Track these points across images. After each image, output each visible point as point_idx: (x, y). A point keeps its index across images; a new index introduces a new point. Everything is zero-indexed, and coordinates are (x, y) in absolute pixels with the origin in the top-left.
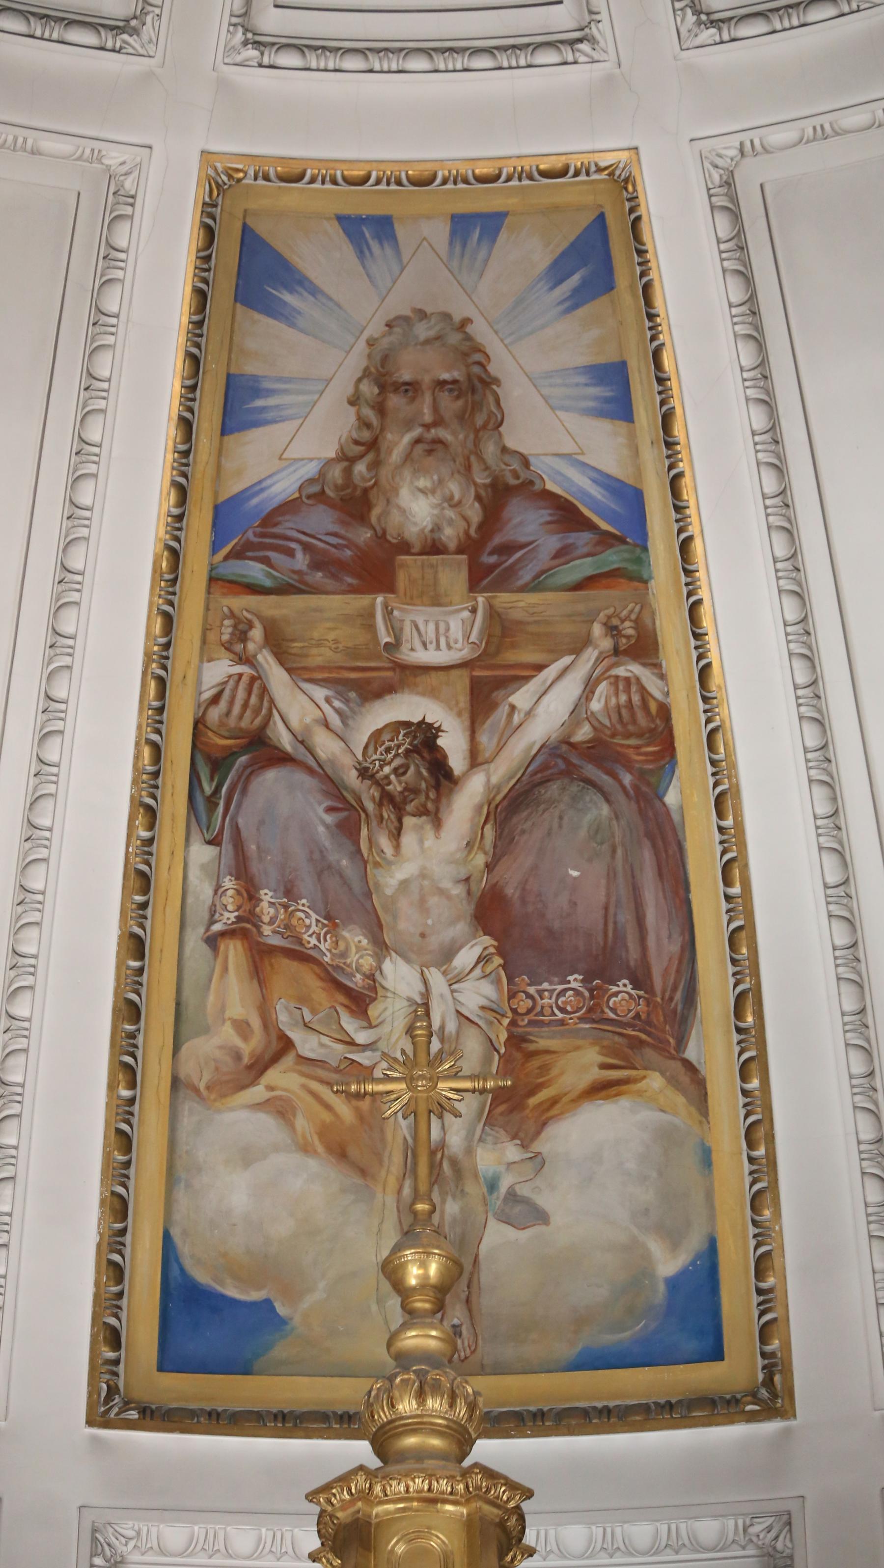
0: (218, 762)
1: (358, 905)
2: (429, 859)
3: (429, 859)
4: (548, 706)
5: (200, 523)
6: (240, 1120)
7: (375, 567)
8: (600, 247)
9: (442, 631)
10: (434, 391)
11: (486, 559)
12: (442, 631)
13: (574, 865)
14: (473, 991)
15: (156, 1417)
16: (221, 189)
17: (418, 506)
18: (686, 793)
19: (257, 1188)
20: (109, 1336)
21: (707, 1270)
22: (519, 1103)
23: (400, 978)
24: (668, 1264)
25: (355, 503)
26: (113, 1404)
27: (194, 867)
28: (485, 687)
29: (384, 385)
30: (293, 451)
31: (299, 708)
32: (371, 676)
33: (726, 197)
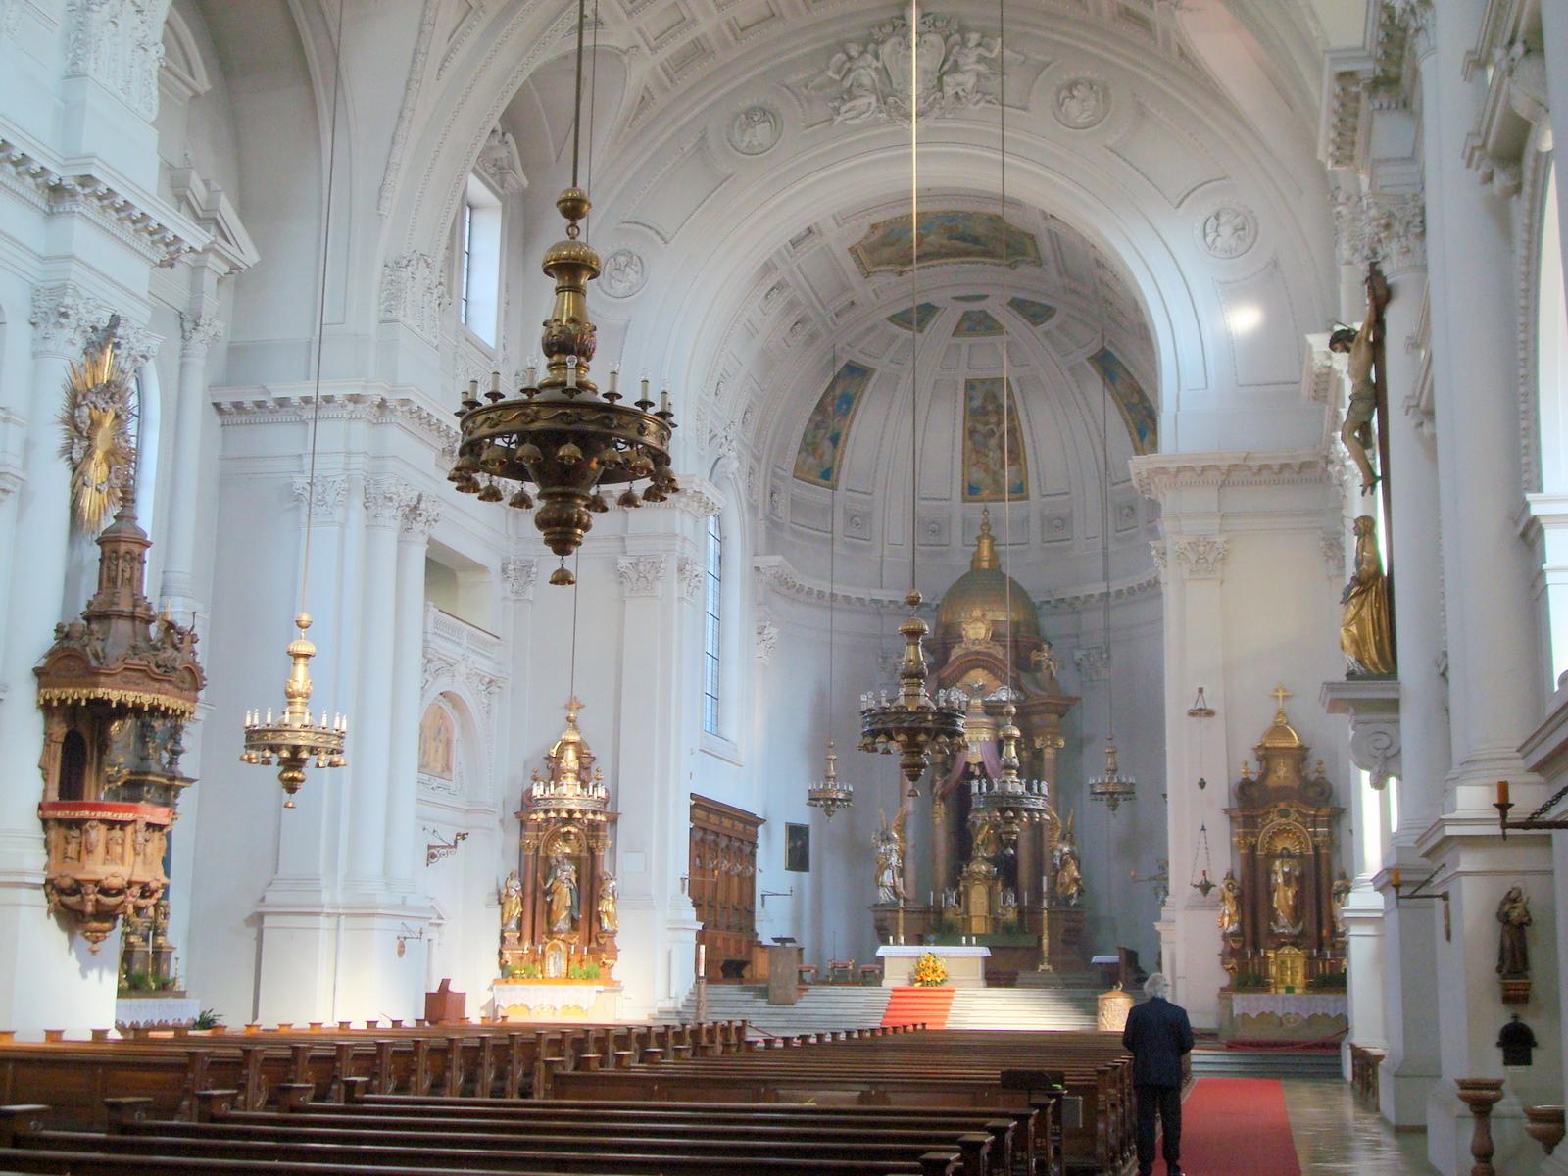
0: (971, 433)
1: (985, 446)
5: (968, 413)
6: (974, 470)
10: (992, 397)
15: (970, 501)
16: (967, 381)
17: (990, 408)
18: (1018, 435)
19: (978, 475)
20: (963, 493)
21: (1022, 483)
23: (991, 454)
24: (1019, 482)
25: (984, 408)
26: (964, 500)
27: (969, 443)
29: (985, 399)
30: (977, 403)
31: (979, 427)
32: (987, 424)
33: (1018, 380)
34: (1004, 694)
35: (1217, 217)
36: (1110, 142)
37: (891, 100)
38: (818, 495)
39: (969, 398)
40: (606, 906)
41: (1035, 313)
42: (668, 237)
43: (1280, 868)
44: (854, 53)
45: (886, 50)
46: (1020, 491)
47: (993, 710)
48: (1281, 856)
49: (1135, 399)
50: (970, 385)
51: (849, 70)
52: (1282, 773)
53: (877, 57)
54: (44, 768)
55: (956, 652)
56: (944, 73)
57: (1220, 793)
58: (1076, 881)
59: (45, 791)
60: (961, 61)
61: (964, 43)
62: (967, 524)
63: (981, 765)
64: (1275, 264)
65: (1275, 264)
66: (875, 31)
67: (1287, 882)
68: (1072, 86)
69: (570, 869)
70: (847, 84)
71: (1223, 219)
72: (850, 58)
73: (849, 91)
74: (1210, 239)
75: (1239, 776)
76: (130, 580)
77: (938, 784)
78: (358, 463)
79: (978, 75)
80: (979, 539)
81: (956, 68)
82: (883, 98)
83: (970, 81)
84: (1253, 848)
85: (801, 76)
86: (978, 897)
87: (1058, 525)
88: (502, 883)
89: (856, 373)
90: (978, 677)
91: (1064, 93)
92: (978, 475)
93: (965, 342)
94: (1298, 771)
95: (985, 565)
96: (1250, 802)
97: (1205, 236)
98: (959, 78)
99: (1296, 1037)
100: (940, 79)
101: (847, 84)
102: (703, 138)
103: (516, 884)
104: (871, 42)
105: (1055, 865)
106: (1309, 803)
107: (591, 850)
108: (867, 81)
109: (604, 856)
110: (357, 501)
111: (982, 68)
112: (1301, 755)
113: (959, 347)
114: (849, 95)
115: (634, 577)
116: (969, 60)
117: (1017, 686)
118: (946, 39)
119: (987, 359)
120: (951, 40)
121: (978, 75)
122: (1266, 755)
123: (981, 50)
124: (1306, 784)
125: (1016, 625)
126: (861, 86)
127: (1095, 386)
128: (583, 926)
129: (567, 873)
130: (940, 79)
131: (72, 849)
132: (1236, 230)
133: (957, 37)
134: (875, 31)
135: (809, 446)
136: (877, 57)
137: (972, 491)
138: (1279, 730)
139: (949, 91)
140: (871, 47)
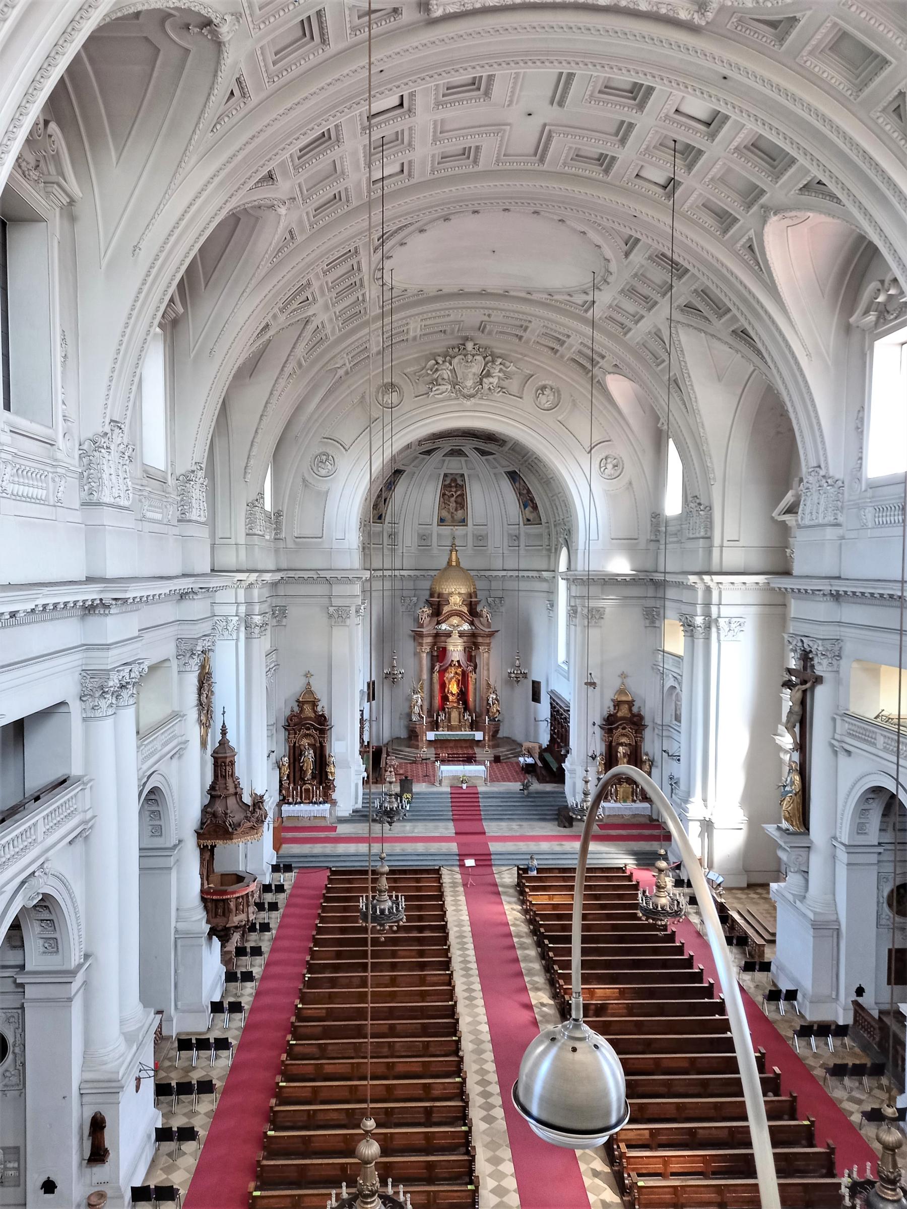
0: (444, 494)
2: (453, 499)
3: (453, 499)
4: (459, 493)
7: (451, 487)
8: (462, 475)
9: (454, 490)
10: (454, 480)
11: (456, 487)
12: (454, 490)
13: (459, 500)
14: (454, 505)
19: (445, 514)
22: (456, 510)
28: (456, 492)
30: (447, 482)
34: (466, 627)
35: (606, 458)
36: (559, 418)
37: (457, 387)
38: (377, 528)
39: (444, 480)
40: (331, 769)
41: (483, 453)
42: (347, 447)
43: (621, 749)
44: (441, 362)
45: (455, 361)
46: (463, 522)
47: (461, 635)
48: (621, 744)
49: (525, 492)
50: (446, 475)
51: (437, 370)
52: (623, 712)
53: (451, 364)
54: (201, 875)
55: (446, 609)
56: (483, 377)
57: (598, 721)
58: (498, 711)
59: (202, 885)
60: (492, 371)
61: (493, 362)
62: (439, 535)
63: (458, 661)
64: (630, 483)
65: (630, 483)
66: (450, 350)
67: (624, 757)
68: (543, 388)
69: (311, 752)
70: (435, 376)
71: (609, 460)
72: (437, 363)
73: (436, 380)
74: (602, 469)
75: (606, 714)
76: (232, 775)
77: (437, 668)
78: (243, 609)
79: (499, 377)
80: (451, 551)
81: (489, 375)
82: (454, 384)
83: (495, 381)
84: (611, 742)
85: (412, 369)
86: (455, 715)
87: (481, 539)
88: (279, 759)
89: (398, 473)
90: (455, 620)
91: (539, 391)
92: (445, 514)
93: (447, 459)
94: (630, 710)
95: (454, 564)
96: (610, 724)
97: (600, 467)
98: (491, 380)
99: (629, 822)
100: (481, 380)
101: (435, 376)
102: (363, 397)
103: (286, 758)
104: (448, 356)
105: (488, 704)
106: (634, 723)
107: (320, 743)
108: (446, 377)
109: (327, 745)
110: (243, 629)
111: (501, 375)
112: (631, 704)
113: (444, 461)
114: (435, 382)
115: (336, 616)
116: (496, 372)
117: (472, 623)
118: (484, 358)
119: (454, 466)
120: (487, 359)
121: (499, 377)
122: (617, 704)
123: (501, 366)
124: (633, 715)
125: (470, 595)
126: (443, 379)
127: (506, 486)
128: (318, 777)
129: (309, 755)
130: (481, 380)
131: (220, 911)
132: (615, 466)
133: (489, 358)
134: (450, 350)
135: (376, 506)
136: (451, 364)
137: (442, 521)
138: (622, 691)
139: (486, 386)
140: (448, 358)
